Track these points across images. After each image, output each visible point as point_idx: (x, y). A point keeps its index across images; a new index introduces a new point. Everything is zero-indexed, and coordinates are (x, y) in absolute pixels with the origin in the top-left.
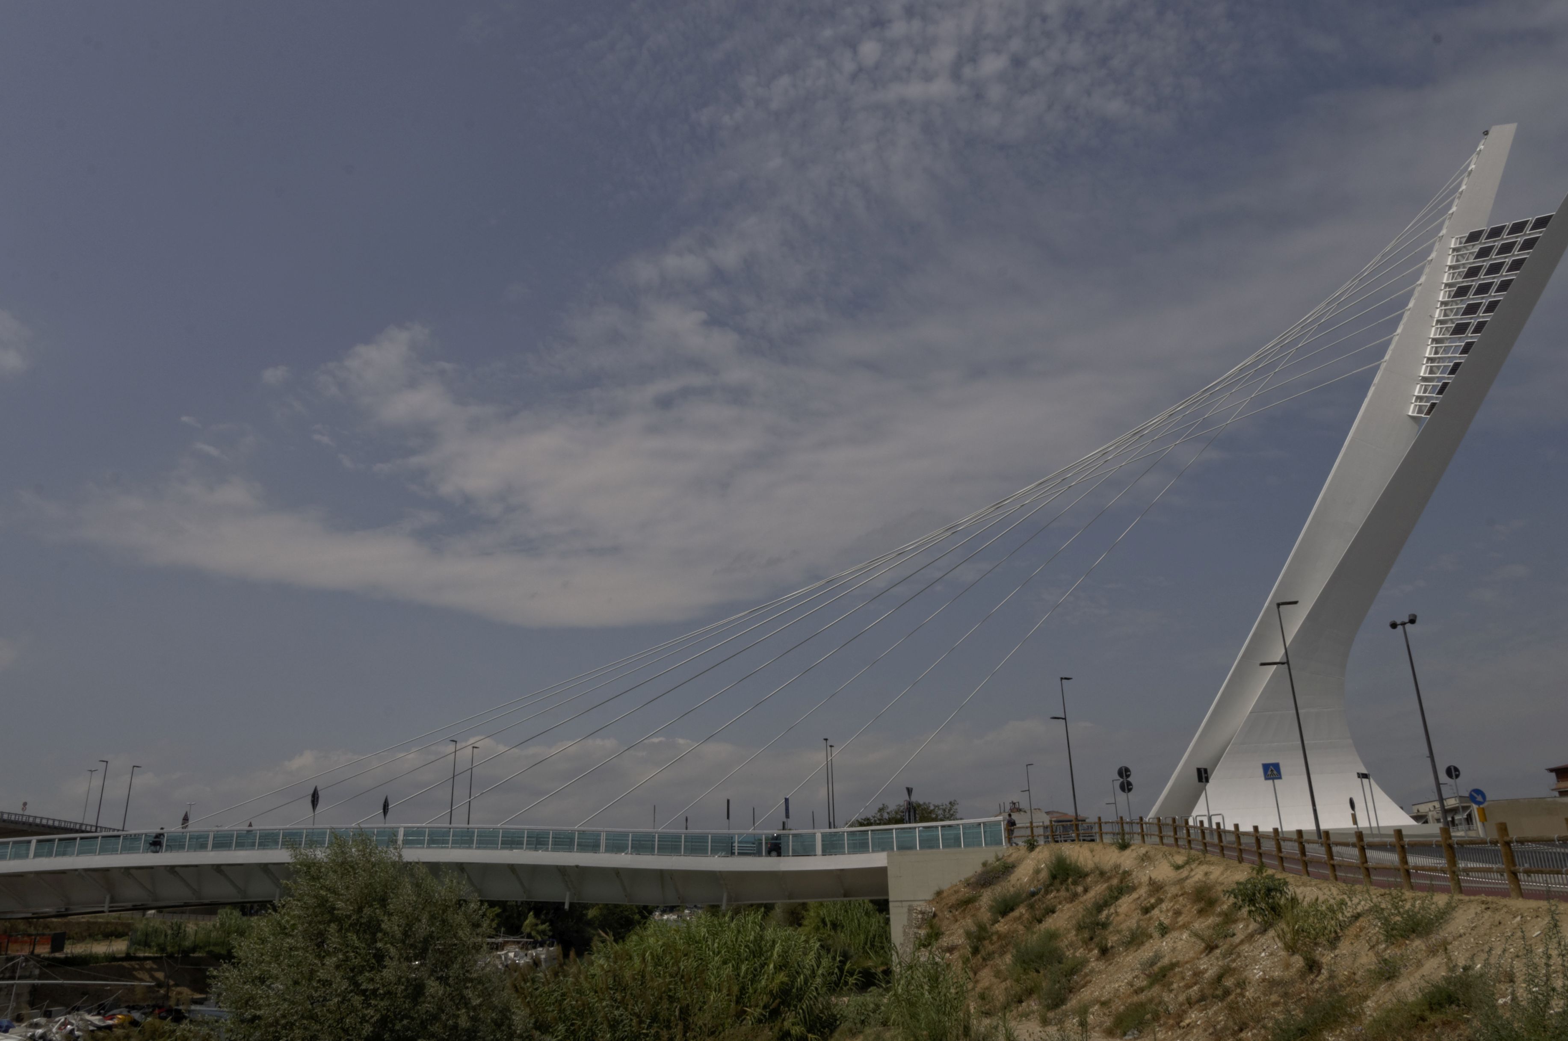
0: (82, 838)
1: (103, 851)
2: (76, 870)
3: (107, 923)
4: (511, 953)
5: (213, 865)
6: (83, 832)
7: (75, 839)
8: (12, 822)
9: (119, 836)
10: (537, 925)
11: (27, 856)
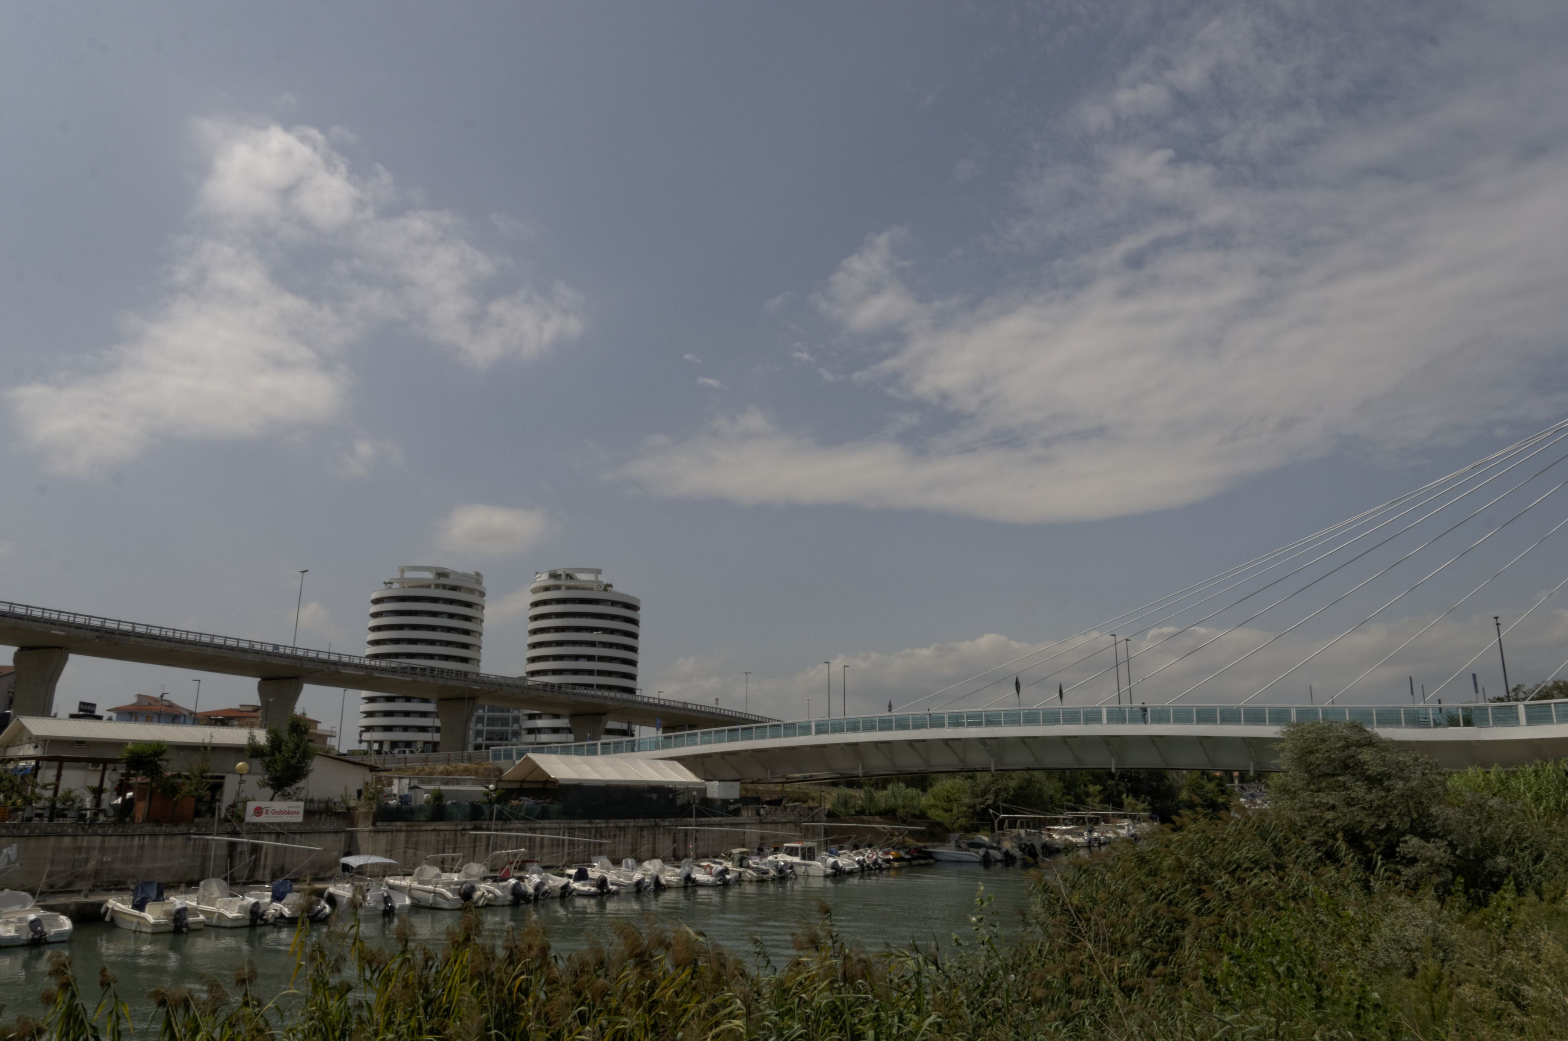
0: (756, 727)
1: (773, 736)
2: (839, 744)
3: (793, 792)
4: (1125, 828)
5: (943, 740)
7: (751, 728)
9: (779, 726)
10: (1136, 805)
11: (810, 734)
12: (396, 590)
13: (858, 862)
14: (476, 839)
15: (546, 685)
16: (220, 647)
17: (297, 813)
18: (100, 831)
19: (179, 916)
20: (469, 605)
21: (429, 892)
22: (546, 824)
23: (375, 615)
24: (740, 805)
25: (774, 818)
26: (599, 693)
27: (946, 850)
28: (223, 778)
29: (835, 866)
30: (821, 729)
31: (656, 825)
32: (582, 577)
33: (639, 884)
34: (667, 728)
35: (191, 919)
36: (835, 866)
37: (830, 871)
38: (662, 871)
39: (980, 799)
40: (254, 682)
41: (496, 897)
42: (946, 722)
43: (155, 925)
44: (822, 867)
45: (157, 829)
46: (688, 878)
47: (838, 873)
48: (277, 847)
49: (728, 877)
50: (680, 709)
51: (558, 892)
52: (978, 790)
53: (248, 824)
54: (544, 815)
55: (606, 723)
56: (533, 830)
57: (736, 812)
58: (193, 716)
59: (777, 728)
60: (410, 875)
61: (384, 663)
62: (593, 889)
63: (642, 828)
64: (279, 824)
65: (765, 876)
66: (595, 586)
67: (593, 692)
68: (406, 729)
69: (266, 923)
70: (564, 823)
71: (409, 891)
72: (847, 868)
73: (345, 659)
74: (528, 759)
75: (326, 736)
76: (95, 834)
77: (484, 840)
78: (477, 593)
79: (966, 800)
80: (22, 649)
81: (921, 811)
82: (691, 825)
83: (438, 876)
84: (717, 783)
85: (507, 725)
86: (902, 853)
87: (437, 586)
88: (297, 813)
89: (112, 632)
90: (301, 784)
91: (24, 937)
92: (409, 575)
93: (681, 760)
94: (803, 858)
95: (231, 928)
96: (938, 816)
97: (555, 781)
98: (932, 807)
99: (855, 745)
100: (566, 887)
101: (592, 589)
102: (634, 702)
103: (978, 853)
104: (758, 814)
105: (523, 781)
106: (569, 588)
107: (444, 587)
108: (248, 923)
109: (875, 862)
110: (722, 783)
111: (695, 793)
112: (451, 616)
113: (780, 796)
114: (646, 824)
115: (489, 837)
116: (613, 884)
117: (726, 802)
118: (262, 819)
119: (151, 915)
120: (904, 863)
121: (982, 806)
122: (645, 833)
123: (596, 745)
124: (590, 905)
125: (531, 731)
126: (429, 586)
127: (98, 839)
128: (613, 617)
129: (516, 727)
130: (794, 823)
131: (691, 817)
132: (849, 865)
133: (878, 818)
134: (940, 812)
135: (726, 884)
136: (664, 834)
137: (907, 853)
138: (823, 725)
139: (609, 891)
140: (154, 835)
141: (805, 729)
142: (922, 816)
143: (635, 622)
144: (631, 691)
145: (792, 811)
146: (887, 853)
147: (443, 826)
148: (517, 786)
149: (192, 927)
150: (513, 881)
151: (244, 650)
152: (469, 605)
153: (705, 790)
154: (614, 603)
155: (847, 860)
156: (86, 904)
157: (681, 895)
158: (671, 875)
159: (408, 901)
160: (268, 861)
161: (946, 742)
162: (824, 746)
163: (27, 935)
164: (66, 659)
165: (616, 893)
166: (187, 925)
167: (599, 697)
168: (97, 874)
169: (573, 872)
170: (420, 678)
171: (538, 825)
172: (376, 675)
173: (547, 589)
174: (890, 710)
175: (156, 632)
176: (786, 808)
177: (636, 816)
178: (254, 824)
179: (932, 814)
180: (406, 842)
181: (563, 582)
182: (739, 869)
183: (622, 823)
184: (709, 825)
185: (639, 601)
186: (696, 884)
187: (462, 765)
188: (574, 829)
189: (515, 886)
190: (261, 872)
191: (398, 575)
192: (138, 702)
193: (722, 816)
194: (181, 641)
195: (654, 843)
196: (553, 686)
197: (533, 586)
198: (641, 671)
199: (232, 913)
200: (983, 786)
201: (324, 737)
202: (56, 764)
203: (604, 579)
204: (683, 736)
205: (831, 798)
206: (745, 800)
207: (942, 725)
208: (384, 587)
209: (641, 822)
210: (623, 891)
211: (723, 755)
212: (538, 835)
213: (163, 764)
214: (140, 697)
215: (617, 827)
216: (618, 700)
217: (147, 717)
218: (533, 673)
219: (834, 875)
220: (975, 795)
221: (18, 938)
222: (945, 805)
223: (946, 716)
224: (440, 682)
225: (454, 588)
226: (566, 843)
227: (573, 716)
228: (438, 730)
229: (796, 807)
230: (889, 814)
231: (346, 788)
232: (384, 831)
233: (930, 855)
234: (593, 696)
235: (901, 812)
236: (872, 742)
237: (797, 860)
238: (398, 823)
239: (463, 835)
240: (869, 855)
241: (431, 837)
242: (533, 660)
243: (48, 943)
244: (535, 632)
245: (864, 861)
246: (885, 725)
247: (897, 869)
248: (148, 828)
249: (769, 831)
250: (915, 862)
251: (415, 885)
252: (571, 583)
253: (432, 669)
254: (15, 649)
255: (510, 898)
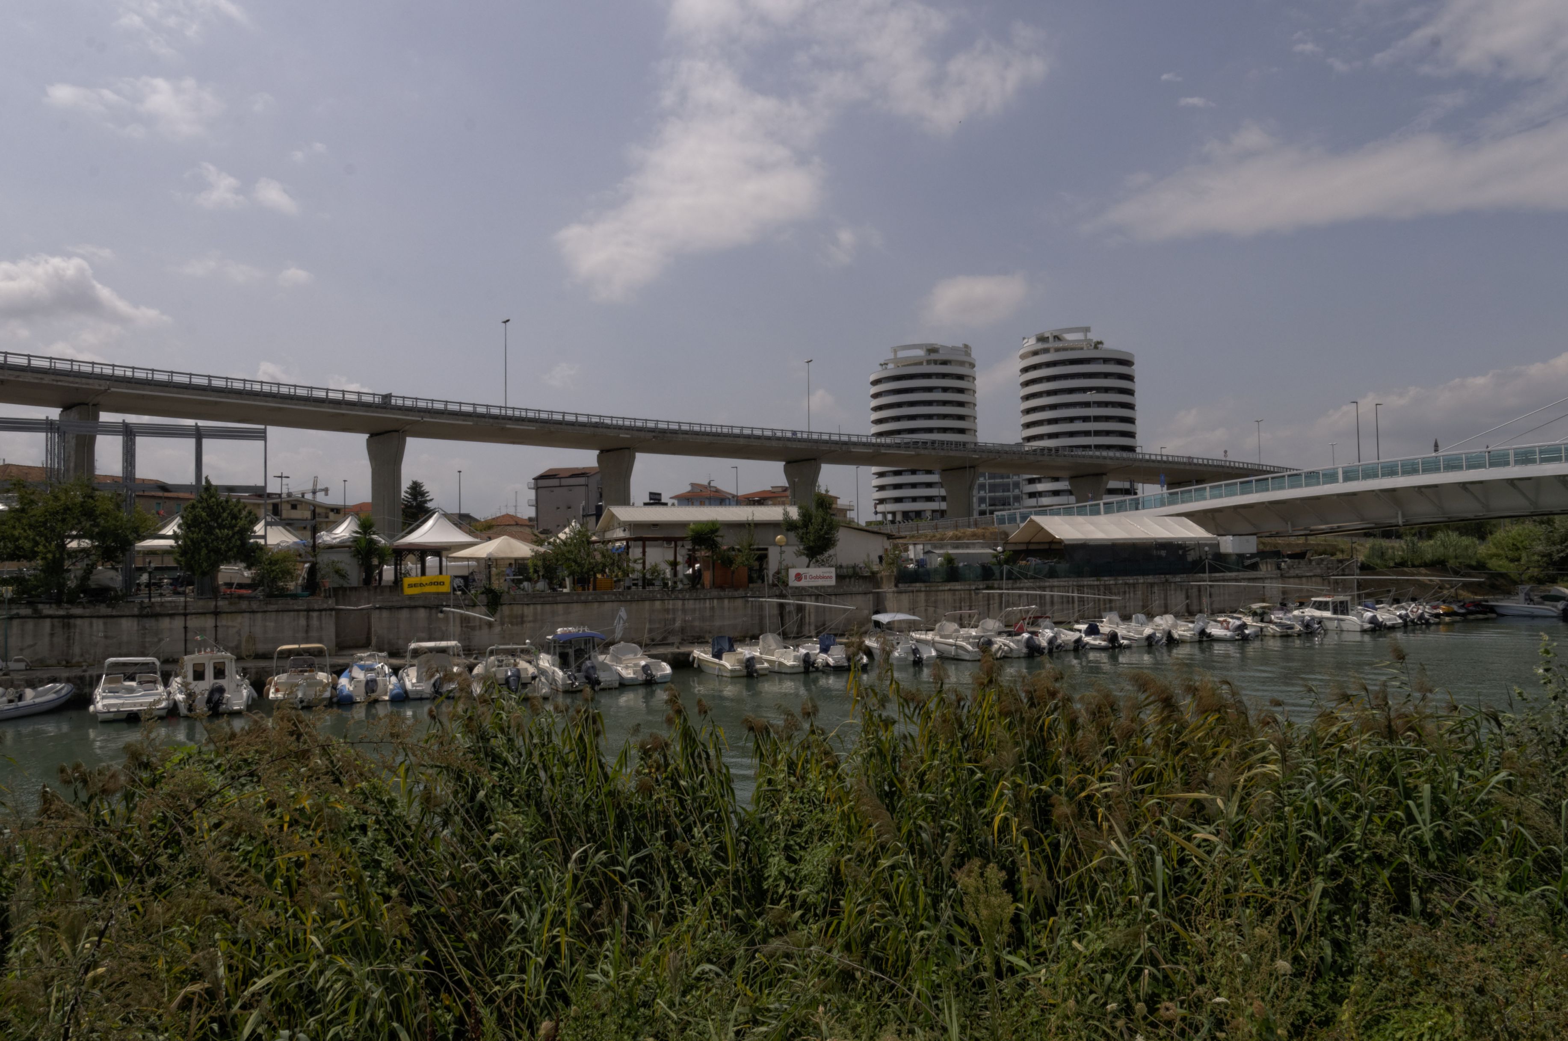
0: (1273, 478)
1: (1292, 487)
2: (1373, 491)
5: (1508, 480)
6: (1274, 472)
8: (1218, 466)
12: (892, 370)
13: (1400, 616)
14: (989, 597)
15: (1043, 449)
16: (748, 437)
17: (830, 577)
18: (680, 596)
19: (750, 663)
20: (960, 377)
21: (951, 645)
22: (1055, 582)
23: (876, 396)
24: (1257, 559)
25: (1297, 572)
26: (1098, 453)
27: (1515, 604)
28: (766, 549)
29: (1373, 620)
30: (1349, 476)
31: (1167, 581)
32: (1069, 337)
33: (1150, 638)
34: (1171, 485)
35: (758, 666)
36: (1373, 620)
37: (1367, 626)
38: (1175, 626)
39: (1559, 547)
40: (780, 465)
41: (1011, 650)
42: (1512, 459)
43: (732, 671)
44: (1358, 622)
45: (722, 594)
46: (1203, 632)
47: (1377, 628)
48: (817, 607)
49: (1247, 632)
50: (1185, 464)
51: (1071, 647)
52: (1556, 536)
53: (792, 588)
54: (1052, 574)
55: (1107, 483)
56: (1043, 588)
57: (1254, 567)
59: (1295, 478)
60: (932, 630)
61: (888, 440)
62: (1103, 643)
63: (1152, 585)
64: (816, 587)
65: (1289, 631)
66: (1084, 345)
67: (1091, 453)
68: (914, 499)
69: (817, 669)
70: (1072, 582)
71: (933, 644)
72: (1388, 623)
73: (854, 439)
74: (1032, 521)
75: (846, 510)
76: (677, 599)
77: (997, 598)
78: (967, 365)
79: (1540, 548)
80: (602, 452)
81: (1478, 562)
82: (1204, 580)
83: (957, 631)
84: (1231, 538)
85: (1009, 491)
86: (1455, 608)
87: (929, 362)
88: (830, 577)
89: (664, 432)
90: (831, 552)
91: (640, 678)
92: (902, 354)
93: (1190, 515)
94: (1335, 612)
95: (791, 674)
96: (1500, 566)
97: (1060, 542)
98: (1492, 556)
99: (1394, 490)
100: (1078, 641)
101: (1082, 349)
102: (1135, 460)
103: (1556, 607)
104: (1279, 568)
105: (1029, 543)
106: (1057, 350)
107: (936, 362)
108: (802, 670)
109: (1421, 617)
110: (1237, 538)
111: (1207, 549)
112: (945, 390)
113: (1303, 549)
114: (1156, 581)
115: (1001, 595)
116: (1123, 638)
117: (1241, 557)
118: (803, 583)
119: (728, 662)
120: (1458, 618)
121: (1562, 554)
122: (1156, 589)
123: (1099, 505)
124: (1103, 657)
125: (1032, 495)
126: (921, 363)
127: (680, 603)
128: (1106, 375)
129: (1017, 492)
130: (1321, 576)
131: (1204, 572)
132: (1390, 620)
133: (1423, 570)
134: (1504, 562)
135: (1245, 639)
136: (1176, 590)
137: (1462, 607)
138: (1352, 471)
139: (1120, 646)
140: (720, 598)
141: (1331, 477)
142: (1481, 567)
143: (1129, 378)
144: (1131, 449)
145: (1318, 564)
146: (1435, 607)
147: (957, 586)
148: (1024, 547)
149: (761, 672)
150: (1026, 635)
151: (768, 438)
152: (960, 377)
153: (1218, 545)
154: (1106, 361)
155: (1387, 614)
156: (679, 654)
157: (1196, 651)
158: (1184, 630)
159: (934, 653)
160: (812, 619)
161: (1512, 482)
162: (1354, 494)
163: (642, 677)
164: (634, 458)
165: (1128, 647)
166: (756, 671)
167: (1098, 457)
168: (683, 630)
169: (1083, 627)
170: (922, 452)
171: (1047, 584)
172: (883, 451)
173: (1035, 353)
174: (1436, 450)
175: (697, 428)
176: (1310, 561)
177: (1144, 573)
178: (796, 588)
179: (1494, 564)
180: (927, 601)
181: (1051, 344)
182: (1260, 624)
183: (1131, 580)
184: (1224, 580)
185: (1133, 356)
186: (1212, 639)
187: (970, 531)
188: (1083, 586)
189: (1029, 640)
190: (807, 628)
191: (892, 356)
193: (1238, 571)
194: (717, 435)
195: (1166, 599)
196: (1050, 449)
197: (1021, 352)
198: (1141, 427)
199: (790, 662)
200: (1563, 530)
201: (844, 511)
202: (640, 543)
203: (1094, 336)
204: (1190, 491)
205: (1363, 549)
206: (1262, 554)
207: (1507, 464)
208: (880, 368)
209: (1150, 579)
210: (1135, 645)
211: (1236, 508)
212: (1048, 593)
213: (719, 539)
214: (693, 485)
215: (1126, 584)
216: (1118, 459)
218: (1029, 439)
219: (1373, 630)
220: (1551, 542)
221: (636, 679)
222: (1511, 554)
223: (1512, 453)
224: (942, 453)
225: (945, 363)
226: (1076, 600)
227: (1072, 478)
228: (944, 499)
229: (1322, 560)
230: (1438, 565)
231: (868, 556)
232: (906, 592)
233: (1492, 609)
234: (1091, 457)
235: (1452, 563)
236: (1414, 487)
237: (1327, 614)
238: (918, 585)
239: (977, 594)
240: (1412, 610)
241: (948, 596)
242: (1028, 425)
243: (657, 683)
244: (1027, 398)
245: (1407, 615)
246: (1431, 467)
247: (1447, 624)
248: (715, 593)
249: (1291, 585)
250: (1471, 617)
251: (937, 639)
252: (1060, 345)
253: (933, 442)
254: (597, 452)
255: (1025, 650)
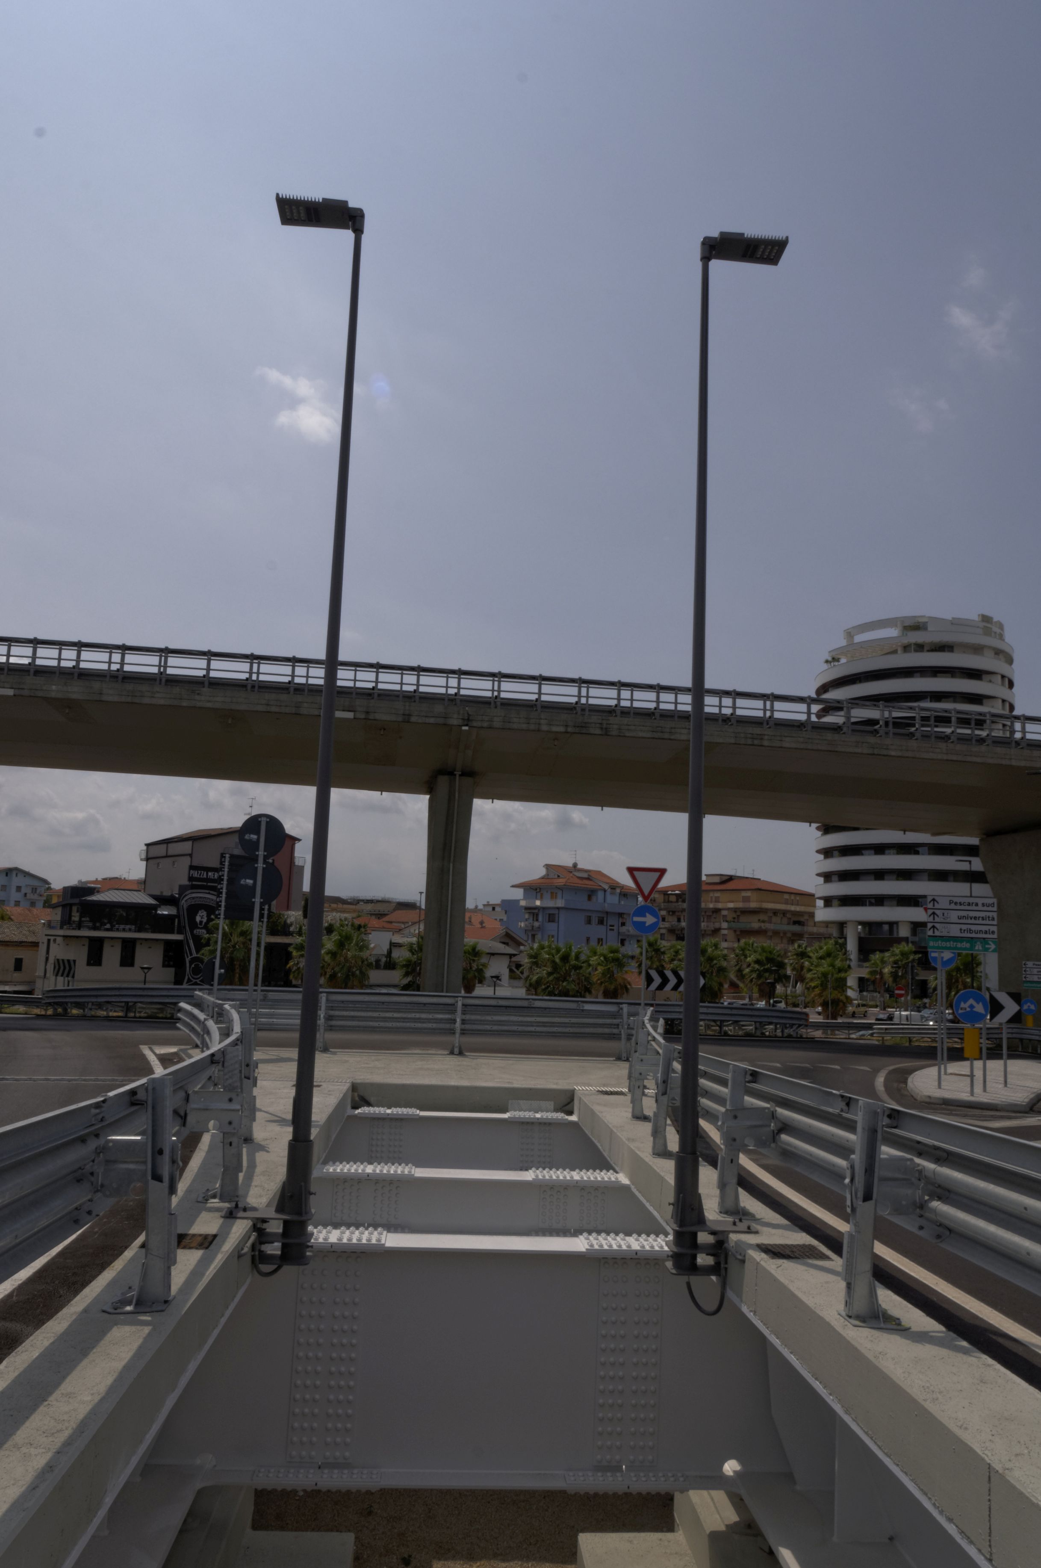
58: (618, 891)
87: (906, 648)
92: (859, 638)
107: (920, 647)
191: (841, 642)
192: (547, 875)
208: (826, 666)
214: (548, 867)
217: (552, 893)
227: (991, 834)
